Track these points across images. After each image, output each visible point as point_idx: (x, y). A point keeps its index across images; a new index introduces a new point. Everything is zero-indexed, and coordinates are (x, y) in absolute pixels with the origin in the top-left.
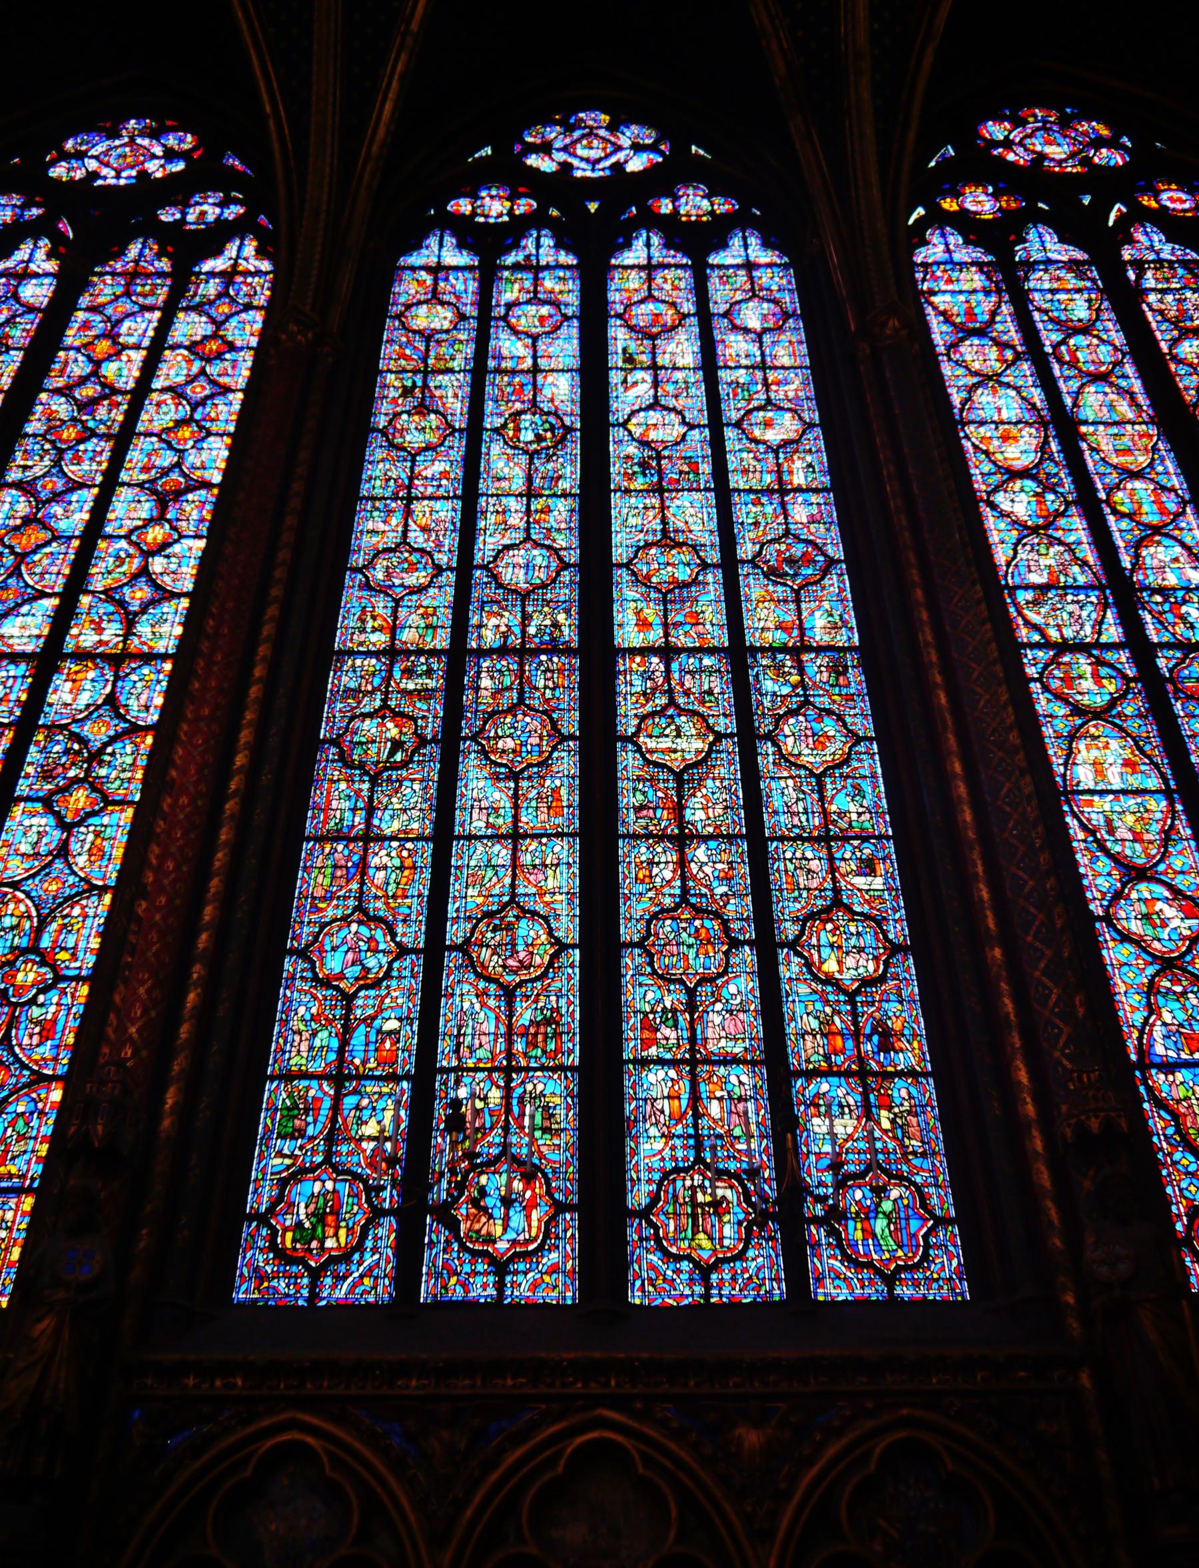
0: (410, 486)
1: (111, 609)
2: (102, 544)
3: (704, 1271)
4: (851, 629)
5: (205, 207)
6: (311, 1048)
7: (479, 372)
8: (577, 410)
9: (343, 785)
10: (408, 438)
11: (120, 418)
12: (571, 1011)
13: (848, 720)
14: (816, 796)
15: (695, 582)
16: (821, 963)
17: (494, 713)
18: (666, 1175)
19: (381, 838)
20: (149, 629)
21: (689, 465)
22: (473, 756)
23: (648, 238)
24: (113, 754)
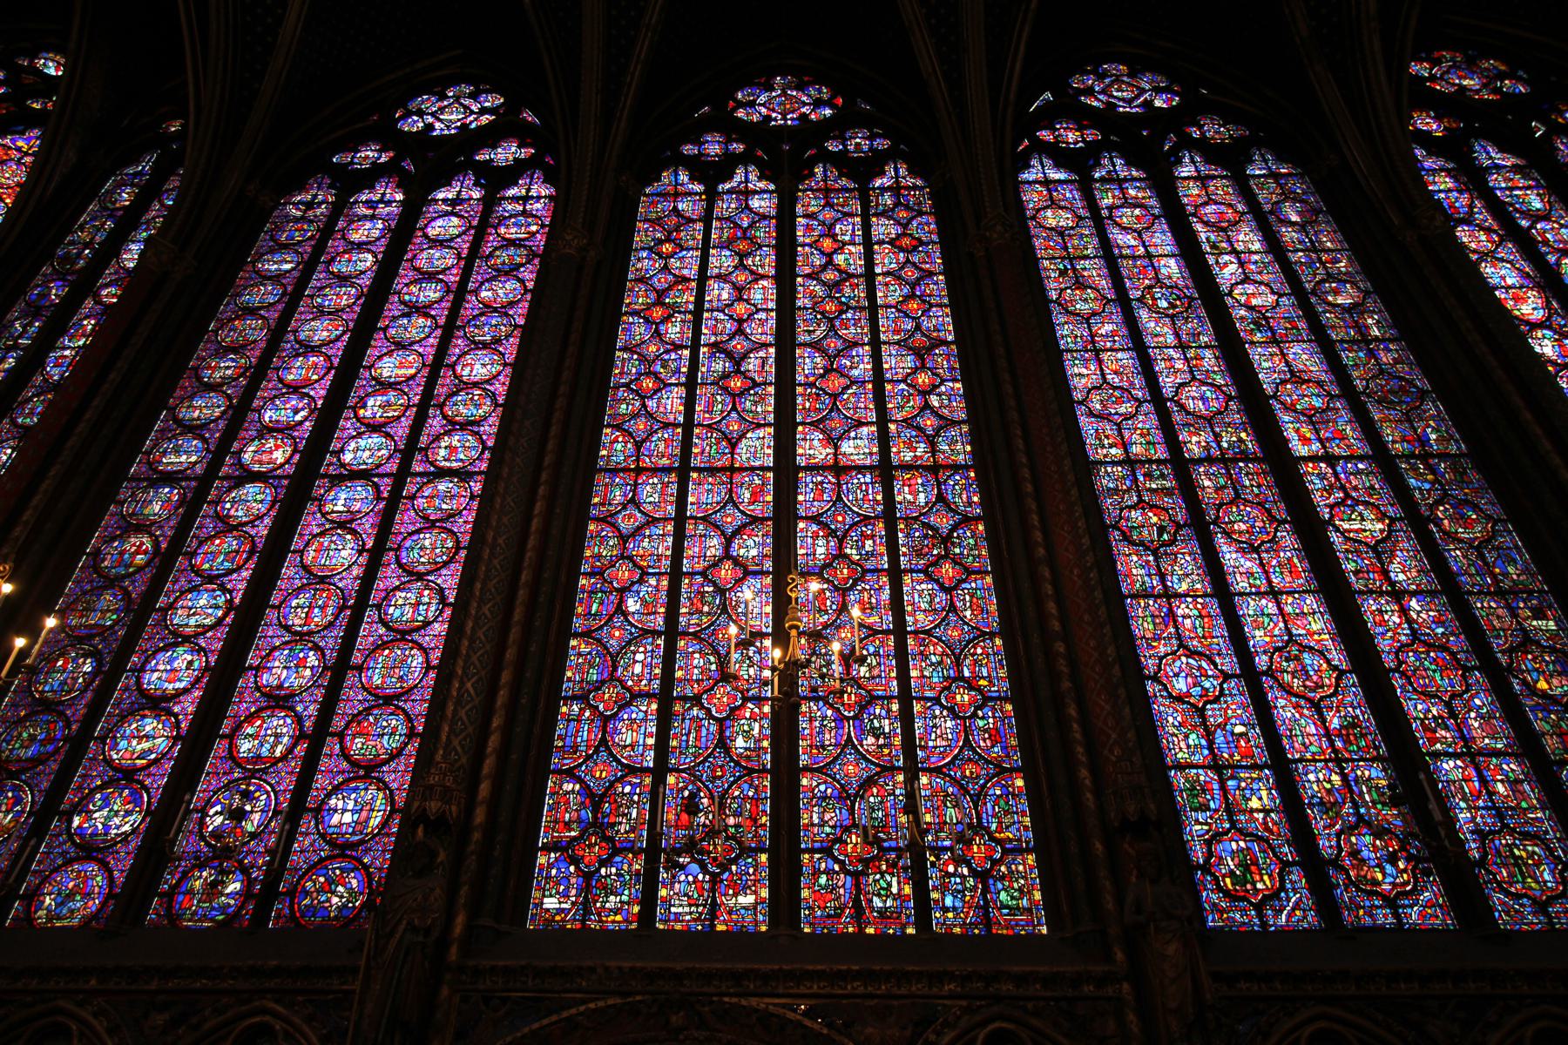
0: (1093, 342)
6: (1188, 747)
9: (1135, 558)
12: (1363, 715)
17: (1221, 505)
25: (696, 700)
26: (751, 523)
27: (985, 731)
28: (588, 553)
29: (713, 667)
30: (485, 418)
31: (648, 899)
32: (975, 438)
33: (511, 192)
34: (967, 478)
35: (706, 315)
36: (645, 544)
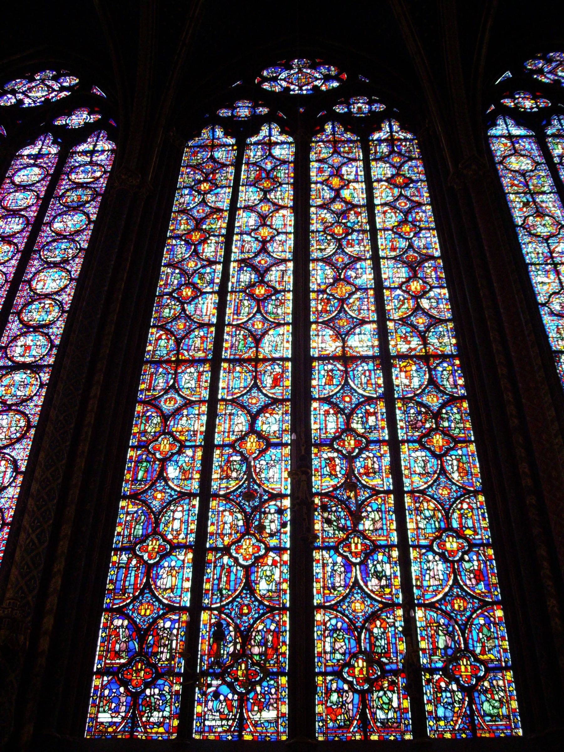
0: (552, 257)
2: (386, 293)
5: (360, 105)
20: (436, 341)
24: (447, 413)
25: (226, 550)
26: (272, 404)
27: (471, 572)
28: (135, 430)
29: (241, 523)
30: (53, 322)
31: (186, 714)
32: (458, 333)
33: (81, 148)
34: (453, 365)
35: (235, 237)
36: (184, 421)
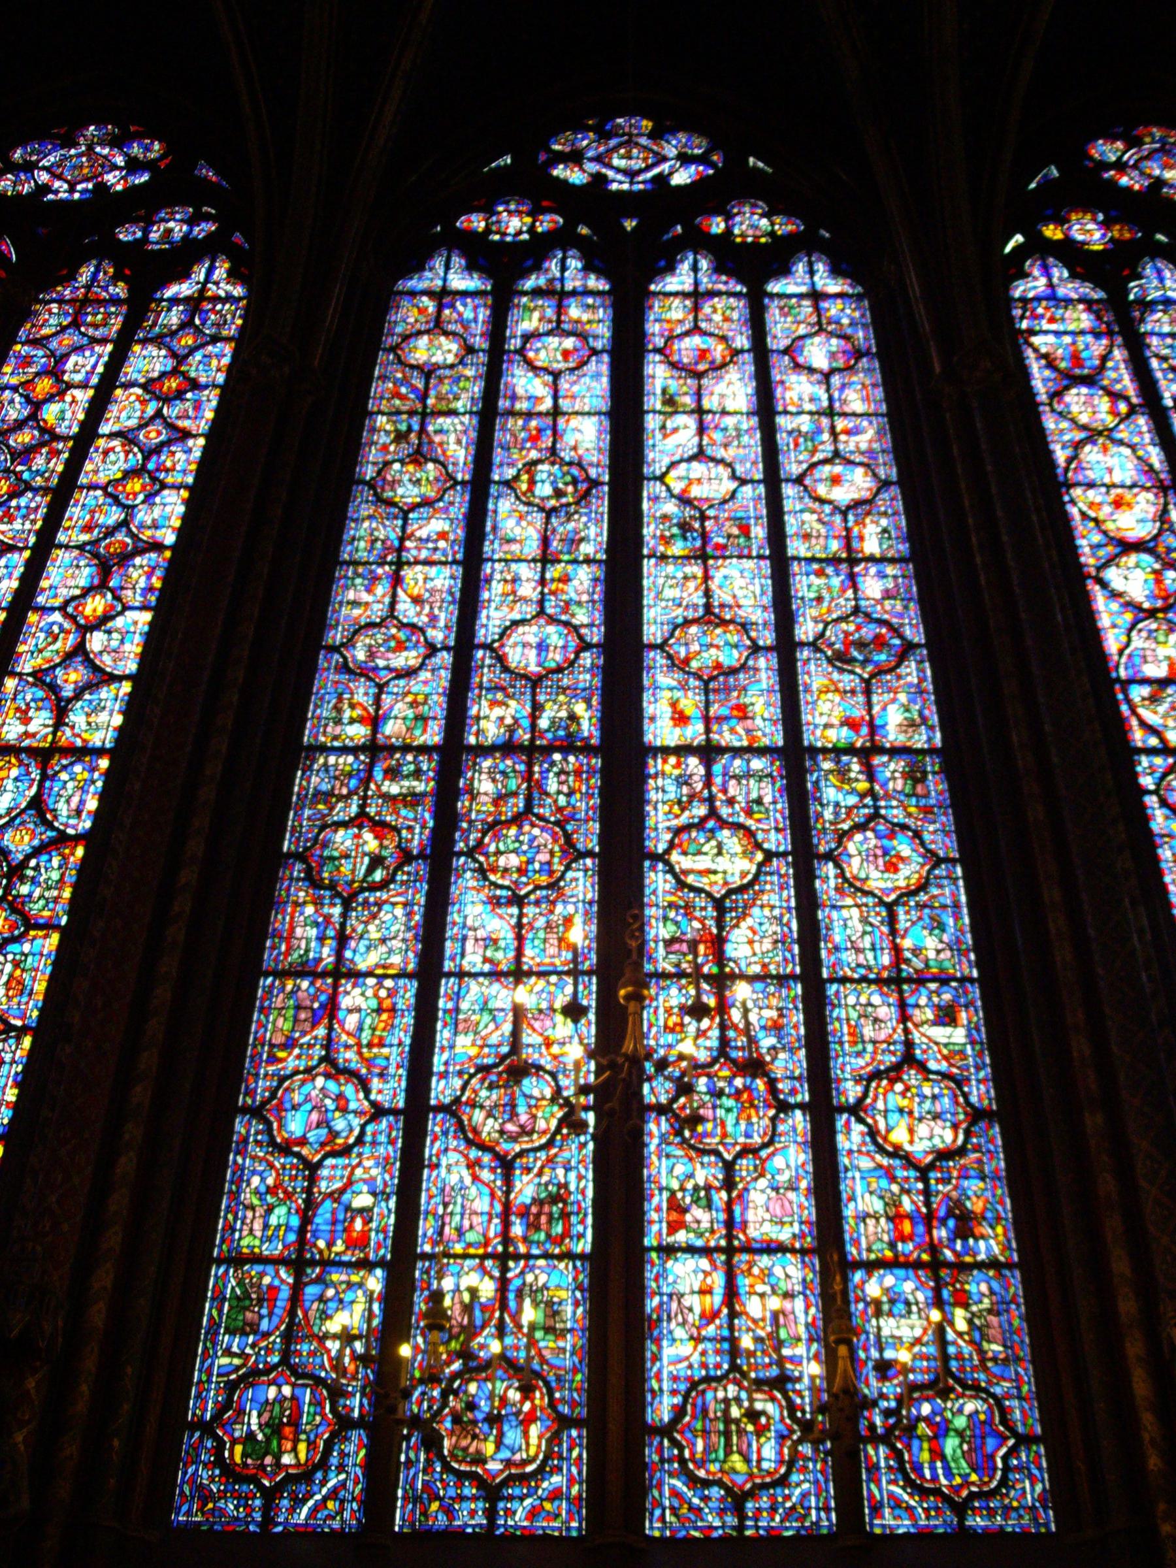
0: (401, 548)
1: (40, 694)
2: (32, 617)
3: (737, 1500)
4: (932, 728)
5: (171, 224)
6: (266, 1226)
7: (488, 414)
8: (606, 461)
9: (310, 910)
10: (400, 491)
11: (60, 468)
12: (582, 1184)
13: (927, 837)
14: (885, 929)
15: (744, 667)
16: (888, 1131)
17: (497, 823)
18: (693, 1384)
19: (356, 975)
21: (740, 527)
22: (468, 875)
23: (696, 262)
34: (92, 770)
